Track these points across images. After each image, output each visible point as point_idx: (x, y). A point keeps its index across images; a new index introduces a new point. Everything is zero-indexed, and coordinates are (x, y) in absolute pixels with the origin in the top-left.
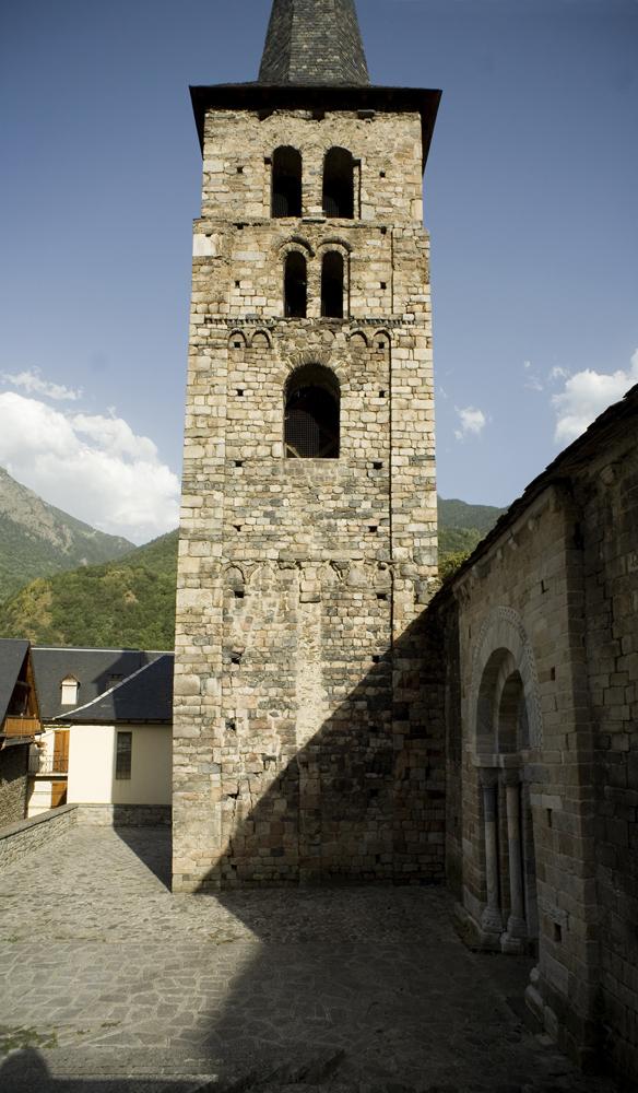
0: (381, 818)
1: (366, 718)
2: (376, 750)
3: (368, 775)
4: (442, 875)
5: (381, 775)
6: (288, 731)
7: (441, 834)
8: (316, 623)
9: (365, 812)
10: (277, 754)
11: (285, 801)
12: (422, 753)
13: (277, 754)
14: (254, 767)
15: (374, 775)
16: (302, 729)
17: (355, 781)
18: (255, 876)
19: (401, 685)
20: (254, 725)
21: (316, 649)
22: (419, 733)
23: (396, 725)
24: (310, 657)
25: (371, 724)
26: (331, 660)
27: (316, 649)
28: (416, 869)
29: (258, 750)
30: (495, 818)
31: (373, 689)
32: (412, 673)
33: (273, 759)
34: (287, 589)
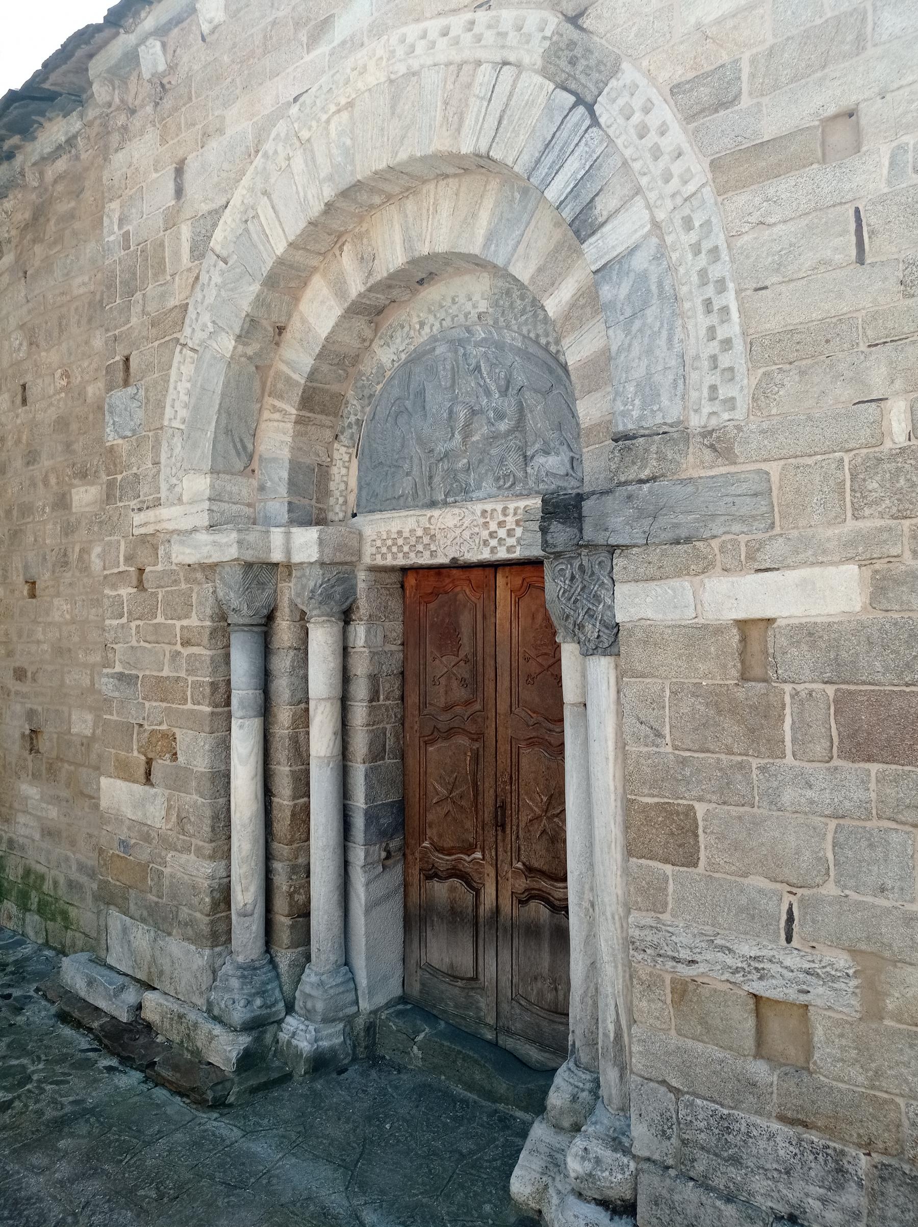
30: (266, 710)
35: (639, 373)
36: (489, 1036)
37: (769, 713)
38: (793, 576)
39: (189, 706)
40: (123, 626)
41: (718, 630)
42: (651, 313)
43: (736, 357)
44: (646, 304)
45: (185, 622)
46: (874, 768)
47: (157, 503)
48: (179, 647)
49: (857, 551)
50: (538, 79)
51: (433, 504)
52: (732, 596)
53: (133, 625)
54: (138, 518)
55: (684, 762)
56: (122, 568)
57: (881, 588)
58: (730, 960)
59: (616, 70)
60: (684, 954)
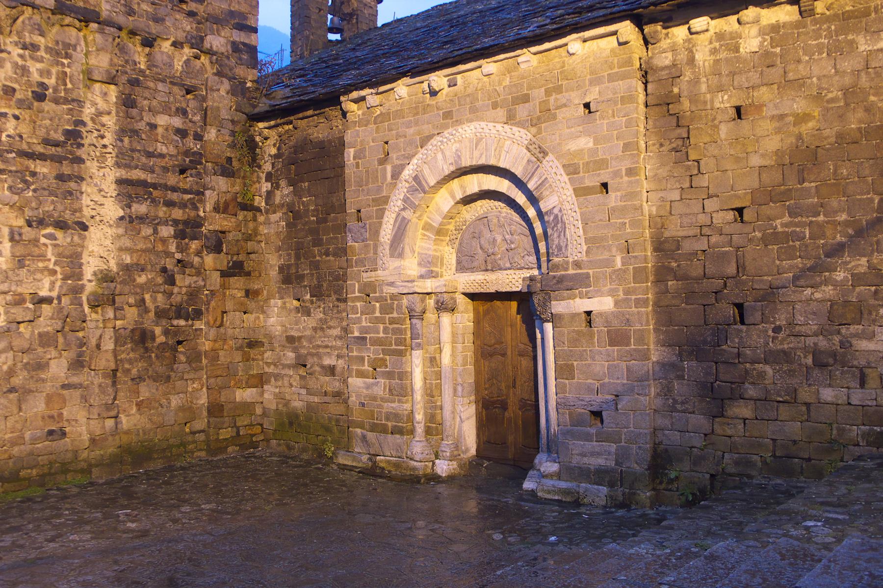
0: (192, 376)
1: (173, 248)
2: (184, 290)
3: (175, 322)
4: (262, 438)
5: (190, 322)
6: (72, 263)
7: (259, 390)
8: (109, 113)
9: (172, 370)
10: (54, 294)
11: (64, 363)
12: (240, 294)
13: (54, 294)
14: (18, 313)
15: (182, 322)
16: (91, 259)
17: (158, 330)
18: (23, 473)
19: (216, 209)
20: (20, 250)
21: (109, 150)
22: (236, 269)
23: (209, 260)
24: (102, 159)
25: (178, 256)
26: (128, 167)
27: (109, 150)
28: (235, 434)
29: (25, 289)
31: (181, 211)
32: (229, 196)
33: (48, 300)
34: (67, 56)
35: (556, 242)
36: (512, 463)
37: (592, 336)
38: (596, 299)
39: (394, 347)
40: (359, 318)
41: (579, 314)
42: (559, 225)
43: (583, 241)
44: (558, 223)
45: (391, 316)
46: (616, 348)
47: (375, 270)
48: (388, 325)
49: (612, 293)
50: (525, 151)
51: (487, 270)
52: (581, 305)
53: (364, 317)
54: (364, 275)
55: (571, 351)
56: (357, 294)
57: (616, 303)
58: (583, 403)
59: (547, 154)
60: (572, 404)
